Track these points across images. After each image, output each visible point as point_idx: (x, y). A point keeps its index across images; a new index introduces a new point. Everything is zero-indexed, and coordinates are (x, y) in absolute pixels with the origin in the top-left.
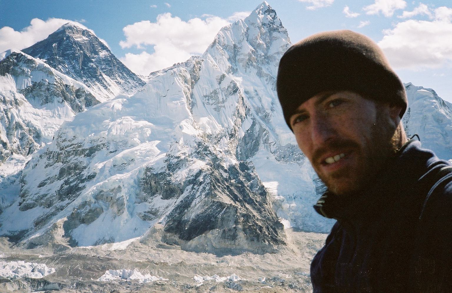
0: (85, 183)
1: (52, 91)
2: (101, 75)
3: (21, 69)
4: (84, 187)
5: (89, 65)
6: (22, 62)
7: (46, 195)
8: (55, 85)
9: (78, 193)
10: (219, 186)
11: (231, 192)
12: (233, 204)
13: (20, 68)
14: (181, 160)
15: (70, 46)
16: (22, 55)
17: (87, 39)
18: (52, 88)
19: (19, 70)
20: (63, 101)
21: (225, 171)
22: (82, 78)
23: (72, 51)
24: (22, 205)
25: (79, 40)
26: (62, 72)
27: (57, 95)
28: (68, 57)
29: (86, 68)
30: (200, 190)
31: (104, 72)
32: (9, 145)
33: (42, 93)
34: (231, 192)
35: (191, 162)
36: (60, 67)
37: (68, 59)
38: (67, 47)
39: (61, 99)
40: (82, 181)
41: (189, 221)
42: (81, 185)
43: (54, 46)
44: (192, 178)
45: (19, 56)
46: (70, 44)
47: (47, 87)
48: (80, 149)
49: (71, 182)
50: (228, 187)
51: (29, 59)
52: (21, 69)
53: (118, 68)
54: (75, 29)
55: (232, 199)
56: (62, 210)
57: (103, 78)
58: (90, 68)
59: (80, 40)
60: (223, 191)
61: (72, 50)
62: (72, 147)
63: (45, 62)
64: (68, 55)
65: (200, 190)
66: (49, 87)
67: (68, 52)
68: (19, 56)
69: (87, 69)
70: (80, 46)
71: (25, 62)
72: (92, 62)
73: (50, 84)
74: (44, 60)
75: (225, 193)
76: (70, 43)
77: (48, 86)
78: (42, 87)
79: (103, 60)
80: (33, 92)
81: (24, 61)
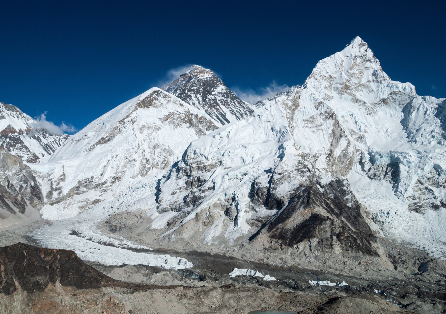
0: (207, 193)
2: (219, 106)
4: (205, 197)
5: (209, 97)
7: (176, 202)
9: (200, 201)
10: (317, 200)
11: (327, 205)
12: (330, 217)
13: (159, 102)
14: (284, 177)
15: (195, 83)
16: (161, 92)
17: (208, 76)
18: (182, 117)
19: (159, 104)
20: (190, 126)
21: (322, 187)
22: (204, 108)
24: (160, 209)
25: (202, 78)
26: (189, 104)
27: (185, 122)
29: (207, 100)
30: (299, 203)
31: (221, 102)
32: (151, 161)
33: (175, 121)
34: (327, 205)
35: (293, 178)
36: (188, 99)
37: (194, 93)
39: (188, 125)
40: (204, 192)
41: (291, 230)
42: (202, 195)
44: (293, 192)
45: (159, 92)
48: (202, 165)
49: (195, 192)
50: (325, 200)
53: (231, 99)
55: (329, 212)
56: (189, 214)
57: (220, 107)
58: (211, 100)
60: (321, 204)
62: (196, 163)
63: (177, 96)
64: (193, 90)
65: (299, 203)
67: (194, 88)
68: (159, 92)
69: (208, 101)
72: (212, 95)
74: (177, 95)
75: (322, 206)
77: (179, 115)
79: (221, 93)
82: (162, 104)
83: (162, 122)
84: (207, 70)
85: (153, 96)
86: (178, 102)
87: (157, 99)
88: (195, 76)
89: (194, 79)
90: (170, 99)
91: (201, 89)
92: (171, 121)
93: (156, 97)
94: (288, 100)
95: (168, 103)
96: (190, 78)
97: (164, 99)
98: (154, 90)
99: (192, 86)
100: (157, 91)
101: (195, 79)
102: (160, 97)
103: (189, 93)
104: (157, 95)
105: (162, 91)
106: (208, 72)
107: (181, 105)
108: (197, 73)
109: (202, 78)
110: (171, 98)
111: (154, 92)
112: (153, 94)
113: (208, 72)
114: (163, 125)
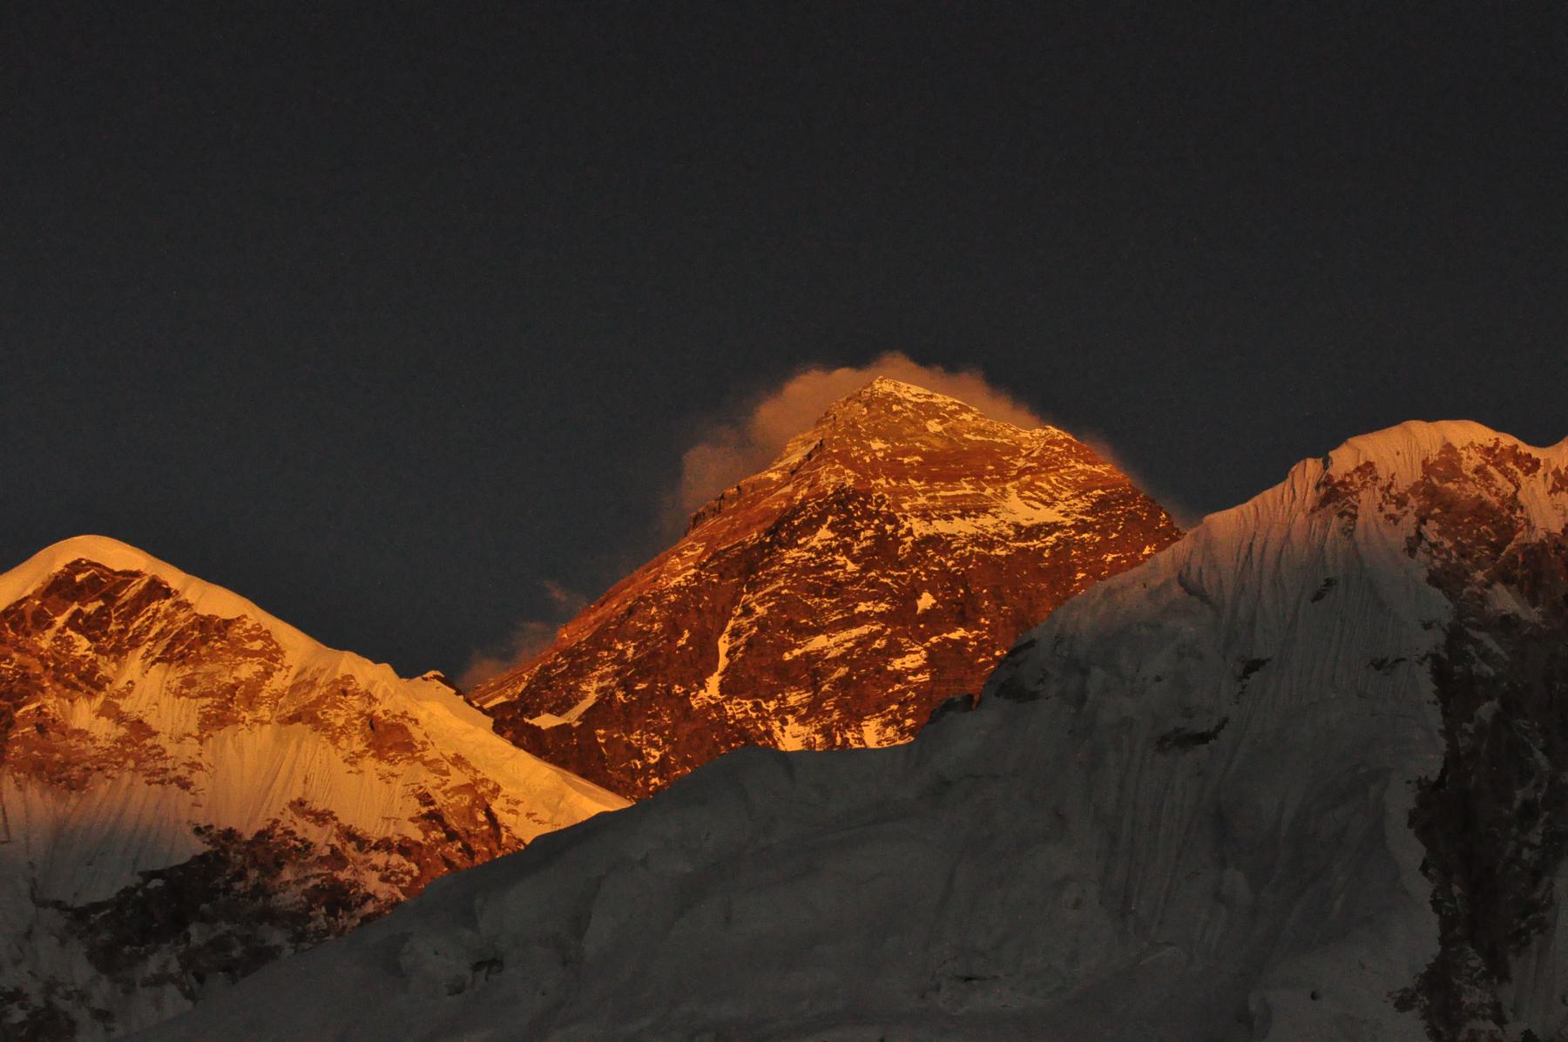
1: (370, 908)
3: (120, 718)
6: (142, 651)
8: (406, 848)
13: (110, 710)
15: (836, 588)
16: (157, 589)
17: (1047, 515)
18: (372, 882)
19: (104, 730)
23: (855, 632)
25: (962, 527)
28: (815, 686)
38: (815, 591)
43: (677, 589)
45: (129, 593)
46: (841, 560)
47: (325, 870)
51: (211, 618)
52: (120, 718)
54: (934, 426)
59: (972, 531)
61: (865, 618)
66: (343, 875)
67: (819, 642)
68: (129, 593)
70: (943, 582)
71: (170, 646)
73: (362, 843)
76: (847, 549)
77: (337, 858)
78: (287, 874)
80: (193, 929)
81: (165, 643)
82: (140, 728)
83: (106, 960)
84: (1035, 436)
85: (45, 641)
86: (355, 702)
87: (91, 682)
88: (843, 498)
89: (824, 533)
90: (247, 670)
91: (913, 659)
92: (219, 945)
93: (82, 645)
94: (1533, 466)
95: (217, 720)
96: (786, 528)
97: (175, 675)
98: (59, 567)
99: (792, 620)
100: (104, 584)
101: (840, 529)
102: (134, 663)
103: (738, 709)
104: (90, 626)
105: (173, 577)
106: (1046, 464)
107: (389, 738)
108: (899, 473)
109: (962, 527)
110: (272, 655)
111: (62, 588)
112: (42, 621)
113: (1046, 464)
114: (104, 992)
